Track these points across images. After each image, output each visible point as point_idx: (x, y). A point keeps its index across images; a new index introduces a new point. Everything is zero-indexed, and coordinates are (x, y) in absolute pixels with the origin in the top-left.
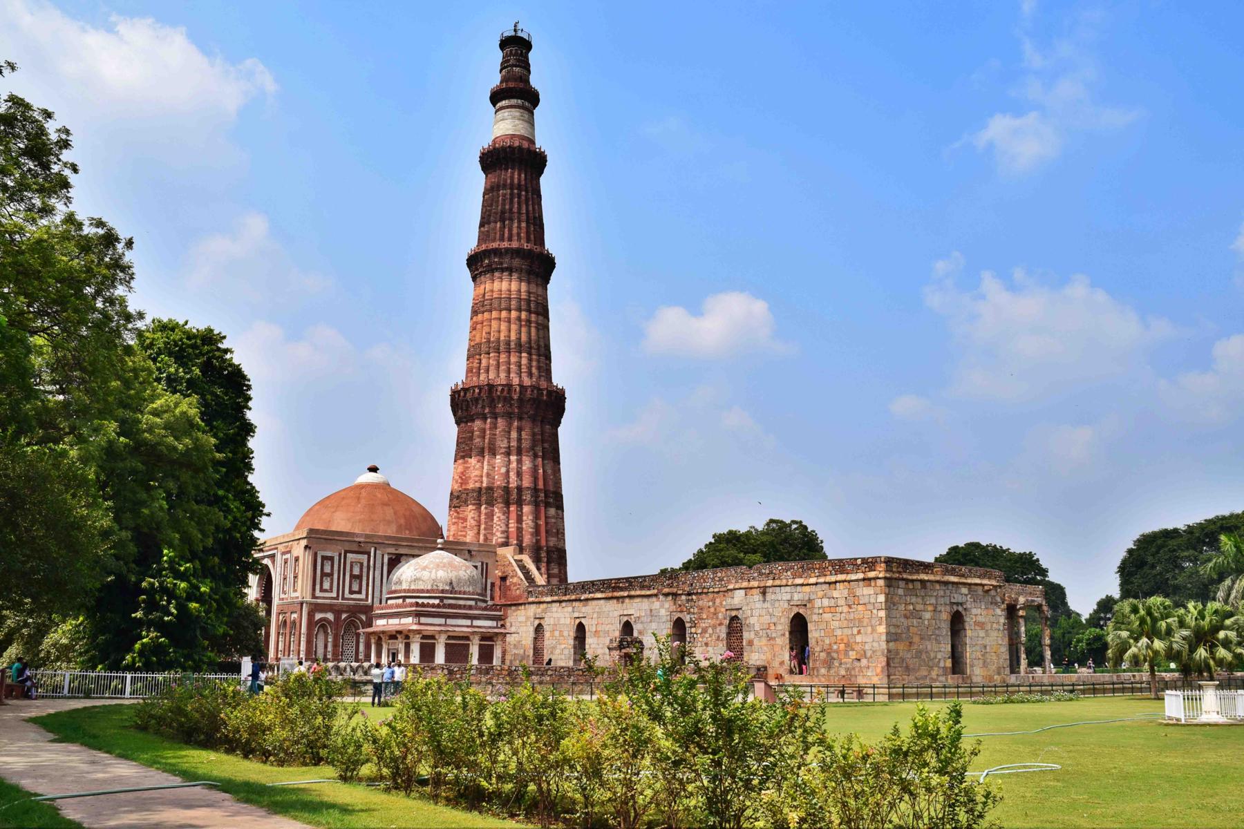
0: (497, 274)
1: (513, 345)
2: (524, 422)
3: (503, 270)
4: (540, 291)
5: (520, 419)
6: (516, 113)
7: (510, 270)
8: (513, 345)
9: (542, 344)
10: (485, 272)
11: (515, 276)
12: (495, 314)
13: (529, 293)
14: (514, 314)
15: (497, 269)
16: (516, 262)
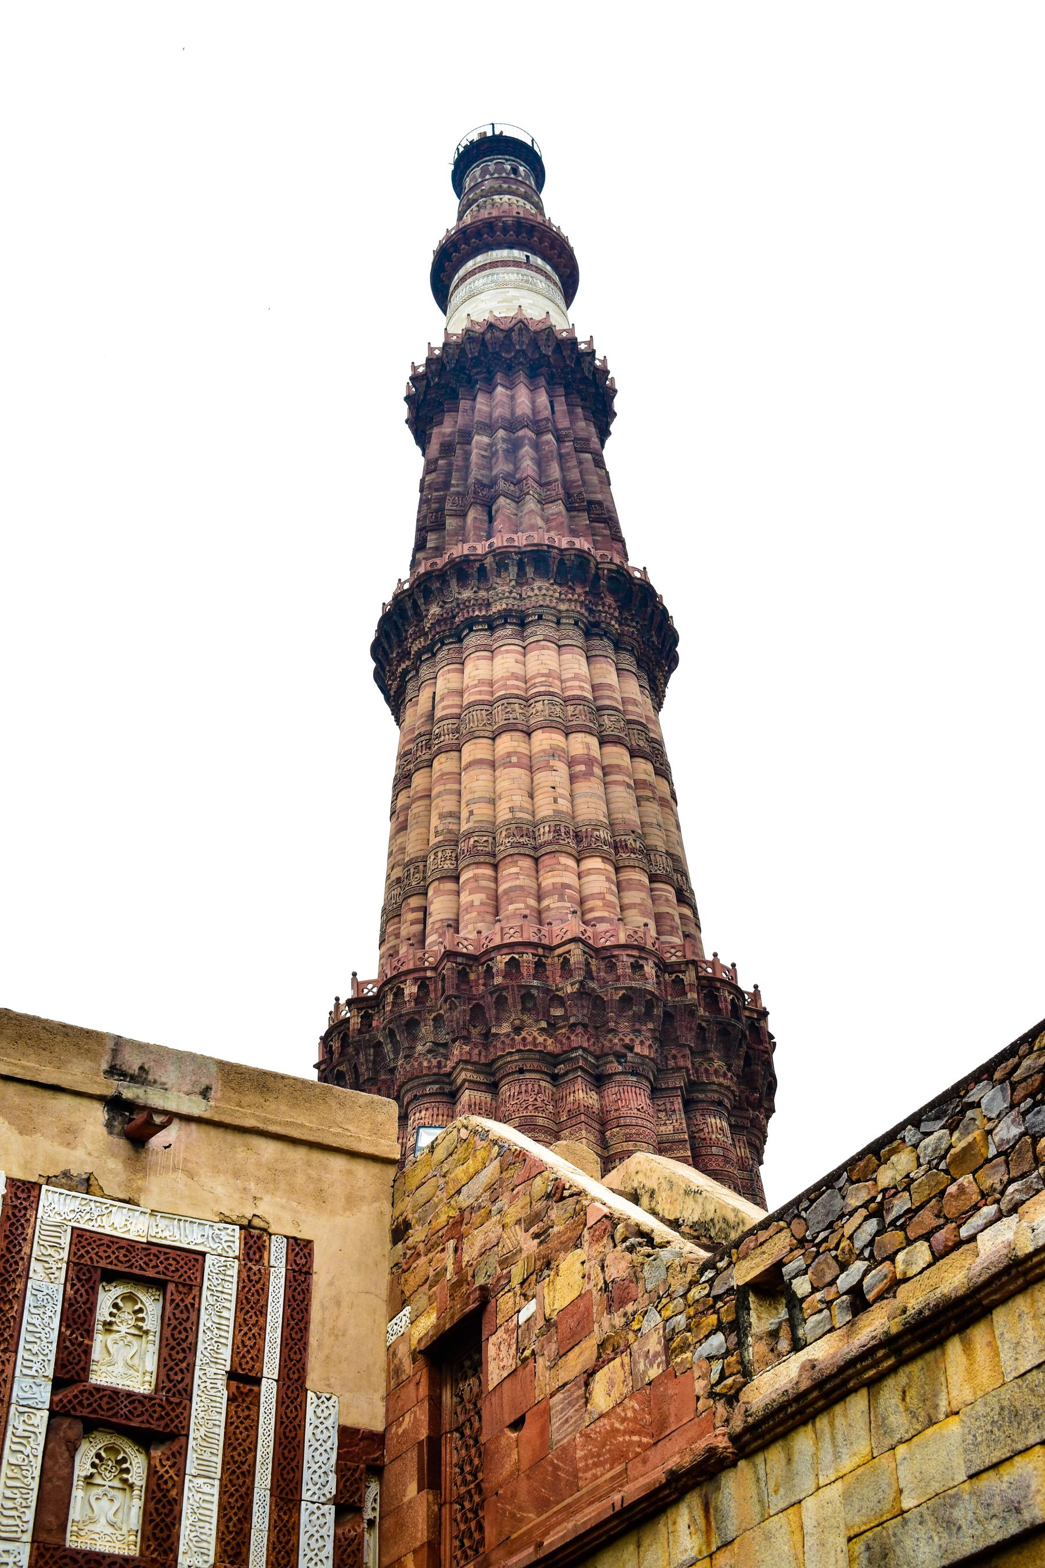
0: (472, 640)
1: (545, 834)
2: (612, 1091)
3: (491, 625)
4: (633, 688)
5: (599, 1081)
6: (511, 275)
7: (520, 621)
8: (545, 834)
9: (656, 840)
10: (431, 651)
11: (539, 631)
12: (473, 750)
13: (594, 688)
14: (543, 740)
15: (470, 624)
16: (541, 592)
